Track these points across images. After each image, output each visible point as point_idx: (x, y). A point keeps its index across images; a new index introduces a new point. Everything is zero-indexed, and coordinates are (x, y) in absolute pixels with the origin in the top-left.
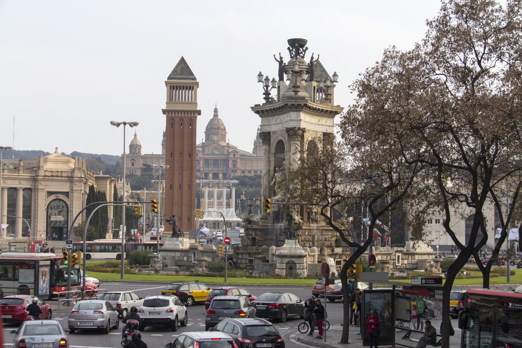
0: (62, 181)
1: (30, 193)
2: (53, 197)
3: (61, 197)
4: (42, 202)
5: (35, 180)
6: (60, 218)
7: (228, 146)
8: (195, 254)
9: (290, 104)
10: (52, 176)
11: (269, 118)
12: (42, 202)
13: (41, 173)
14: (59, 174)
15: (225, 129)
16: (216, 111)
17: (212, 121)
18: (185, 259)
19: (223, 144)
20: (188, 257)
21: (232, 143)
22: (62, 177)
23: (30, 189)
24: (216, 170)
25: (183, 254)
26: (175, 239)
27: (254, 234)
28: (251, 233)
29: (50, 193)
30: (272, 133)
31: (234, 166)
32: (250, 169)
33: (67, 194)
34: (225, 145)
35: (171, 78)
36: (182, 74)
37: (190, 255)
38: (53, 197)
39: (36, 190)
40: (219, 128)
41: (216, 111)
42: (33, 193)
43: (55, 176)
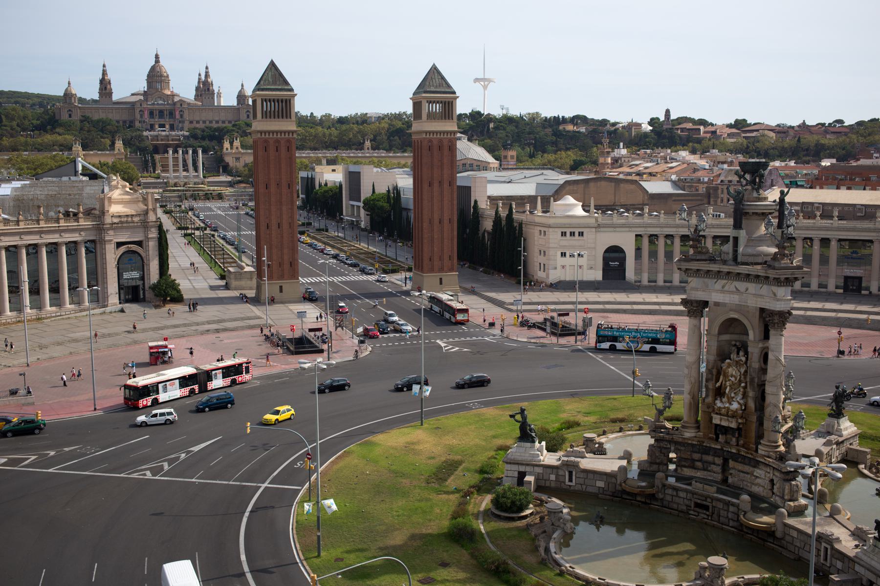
0: (134, 227)
1: (94, 248)
2: (123, 249)
3: (134, 247)
4: (112, 256)
5: (100, 228)
6: (136, 274)
7: (173, 95)
8: (571, 473)
9: (783, 277)
10: (121, 222)
11: (706, 280)
12: (112, 256)
13: (108, 220)
14: (130, 219)
15: (168, 76)
16: (157, 57)
17: (153, 69)
18: (553, 477)
19: (168, 92)
20: (557, 475)
21: (176, 91)
22: (133, 222)
23: (93, 241)
24: (162, 122)
25: (549, 471)
26: (528, 445)
29: (119, 245)
31: (181, 116)
32: (198, 119)
33: (139, 243)
34: (169, 93)
35: (259, 90)
36: (274, 83)
37: (561, 473)
38: (123, 249)
39: (103, 242)
40: (161, 76)
41: (157, 57)
42: (98, 246)
43: (123, 223)
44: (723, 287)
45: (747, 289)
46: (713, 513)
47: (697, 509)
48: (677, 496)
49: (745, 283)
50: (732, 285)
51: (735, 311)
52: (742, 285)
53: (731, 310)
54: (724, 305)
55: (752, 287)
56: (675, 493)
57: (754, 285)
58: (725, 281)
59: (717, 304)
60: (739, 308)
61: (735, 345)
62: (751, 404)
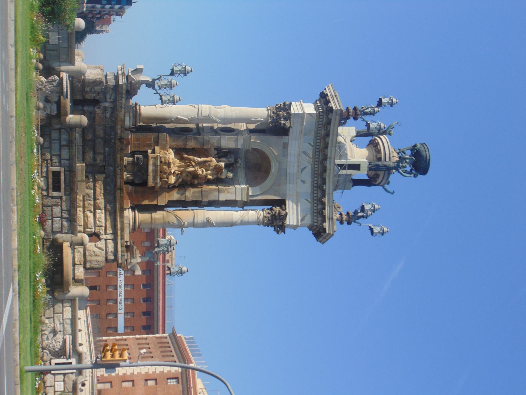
11: (313, 133)
27: (107, 105)
28: (108, 100)
30: (285, 139)
44: (305, 153)
45: (303, 182)
46: (52, 197)
47: (50, 176)
48: (61, 146)
49: (310, 180)
50: (307, 162)
51: (280, 169)
52: (307, 175)
53: (280, 163)
54: (285, 154)
55: (306, 188)
56: (64, 143)
57: (309, 190)
58: (311, 154)
59: (285, 146)
60: (283, 173)
61: (236, 162)
62: (175, 196)
